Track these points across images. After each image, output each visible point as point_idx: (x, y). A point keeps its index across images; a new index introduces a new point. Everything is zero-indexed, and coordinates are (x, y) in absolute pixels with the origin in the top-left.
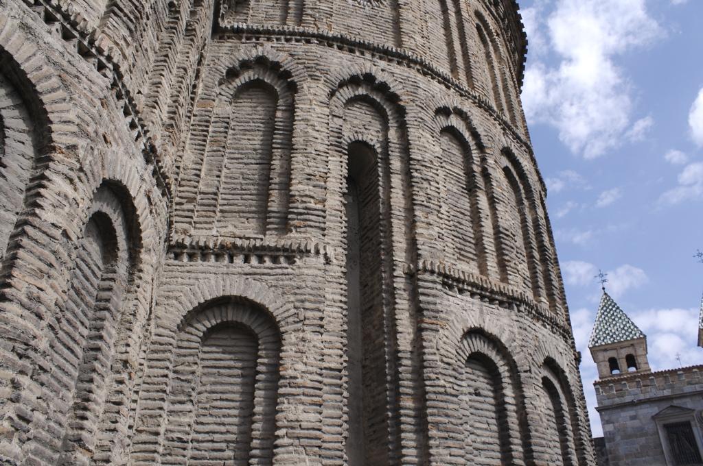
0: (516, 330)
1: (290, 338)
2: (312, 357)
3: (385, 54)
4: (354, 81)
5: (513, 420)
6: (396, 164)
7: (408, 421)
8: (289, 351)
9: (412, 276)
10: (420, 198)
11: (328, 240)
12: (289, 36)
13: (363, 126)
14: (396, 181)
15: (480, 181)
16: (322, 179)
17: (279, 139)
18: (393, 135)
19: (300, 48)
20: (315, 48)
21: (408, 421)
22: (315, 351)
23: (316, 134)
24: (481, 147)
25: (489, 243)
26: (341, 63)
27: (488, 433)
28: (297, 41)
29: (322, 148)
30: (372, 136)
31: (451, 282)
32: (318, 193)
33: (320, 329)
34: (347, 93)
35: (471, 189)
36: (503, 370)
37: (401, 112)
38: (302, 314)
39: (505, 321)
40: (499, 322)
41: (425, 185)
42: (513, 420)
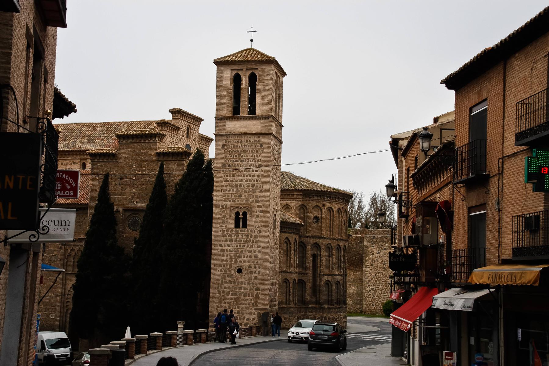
9: (320, 275)
11: (310, 272)
16: (310, 260)
19: (307, 239)
22: (309, 285)
25: (331, 266)
26: (312, 241)
27: (326, 292)
31: (324, 275)
37: (320, 248)
40: (330, 279)
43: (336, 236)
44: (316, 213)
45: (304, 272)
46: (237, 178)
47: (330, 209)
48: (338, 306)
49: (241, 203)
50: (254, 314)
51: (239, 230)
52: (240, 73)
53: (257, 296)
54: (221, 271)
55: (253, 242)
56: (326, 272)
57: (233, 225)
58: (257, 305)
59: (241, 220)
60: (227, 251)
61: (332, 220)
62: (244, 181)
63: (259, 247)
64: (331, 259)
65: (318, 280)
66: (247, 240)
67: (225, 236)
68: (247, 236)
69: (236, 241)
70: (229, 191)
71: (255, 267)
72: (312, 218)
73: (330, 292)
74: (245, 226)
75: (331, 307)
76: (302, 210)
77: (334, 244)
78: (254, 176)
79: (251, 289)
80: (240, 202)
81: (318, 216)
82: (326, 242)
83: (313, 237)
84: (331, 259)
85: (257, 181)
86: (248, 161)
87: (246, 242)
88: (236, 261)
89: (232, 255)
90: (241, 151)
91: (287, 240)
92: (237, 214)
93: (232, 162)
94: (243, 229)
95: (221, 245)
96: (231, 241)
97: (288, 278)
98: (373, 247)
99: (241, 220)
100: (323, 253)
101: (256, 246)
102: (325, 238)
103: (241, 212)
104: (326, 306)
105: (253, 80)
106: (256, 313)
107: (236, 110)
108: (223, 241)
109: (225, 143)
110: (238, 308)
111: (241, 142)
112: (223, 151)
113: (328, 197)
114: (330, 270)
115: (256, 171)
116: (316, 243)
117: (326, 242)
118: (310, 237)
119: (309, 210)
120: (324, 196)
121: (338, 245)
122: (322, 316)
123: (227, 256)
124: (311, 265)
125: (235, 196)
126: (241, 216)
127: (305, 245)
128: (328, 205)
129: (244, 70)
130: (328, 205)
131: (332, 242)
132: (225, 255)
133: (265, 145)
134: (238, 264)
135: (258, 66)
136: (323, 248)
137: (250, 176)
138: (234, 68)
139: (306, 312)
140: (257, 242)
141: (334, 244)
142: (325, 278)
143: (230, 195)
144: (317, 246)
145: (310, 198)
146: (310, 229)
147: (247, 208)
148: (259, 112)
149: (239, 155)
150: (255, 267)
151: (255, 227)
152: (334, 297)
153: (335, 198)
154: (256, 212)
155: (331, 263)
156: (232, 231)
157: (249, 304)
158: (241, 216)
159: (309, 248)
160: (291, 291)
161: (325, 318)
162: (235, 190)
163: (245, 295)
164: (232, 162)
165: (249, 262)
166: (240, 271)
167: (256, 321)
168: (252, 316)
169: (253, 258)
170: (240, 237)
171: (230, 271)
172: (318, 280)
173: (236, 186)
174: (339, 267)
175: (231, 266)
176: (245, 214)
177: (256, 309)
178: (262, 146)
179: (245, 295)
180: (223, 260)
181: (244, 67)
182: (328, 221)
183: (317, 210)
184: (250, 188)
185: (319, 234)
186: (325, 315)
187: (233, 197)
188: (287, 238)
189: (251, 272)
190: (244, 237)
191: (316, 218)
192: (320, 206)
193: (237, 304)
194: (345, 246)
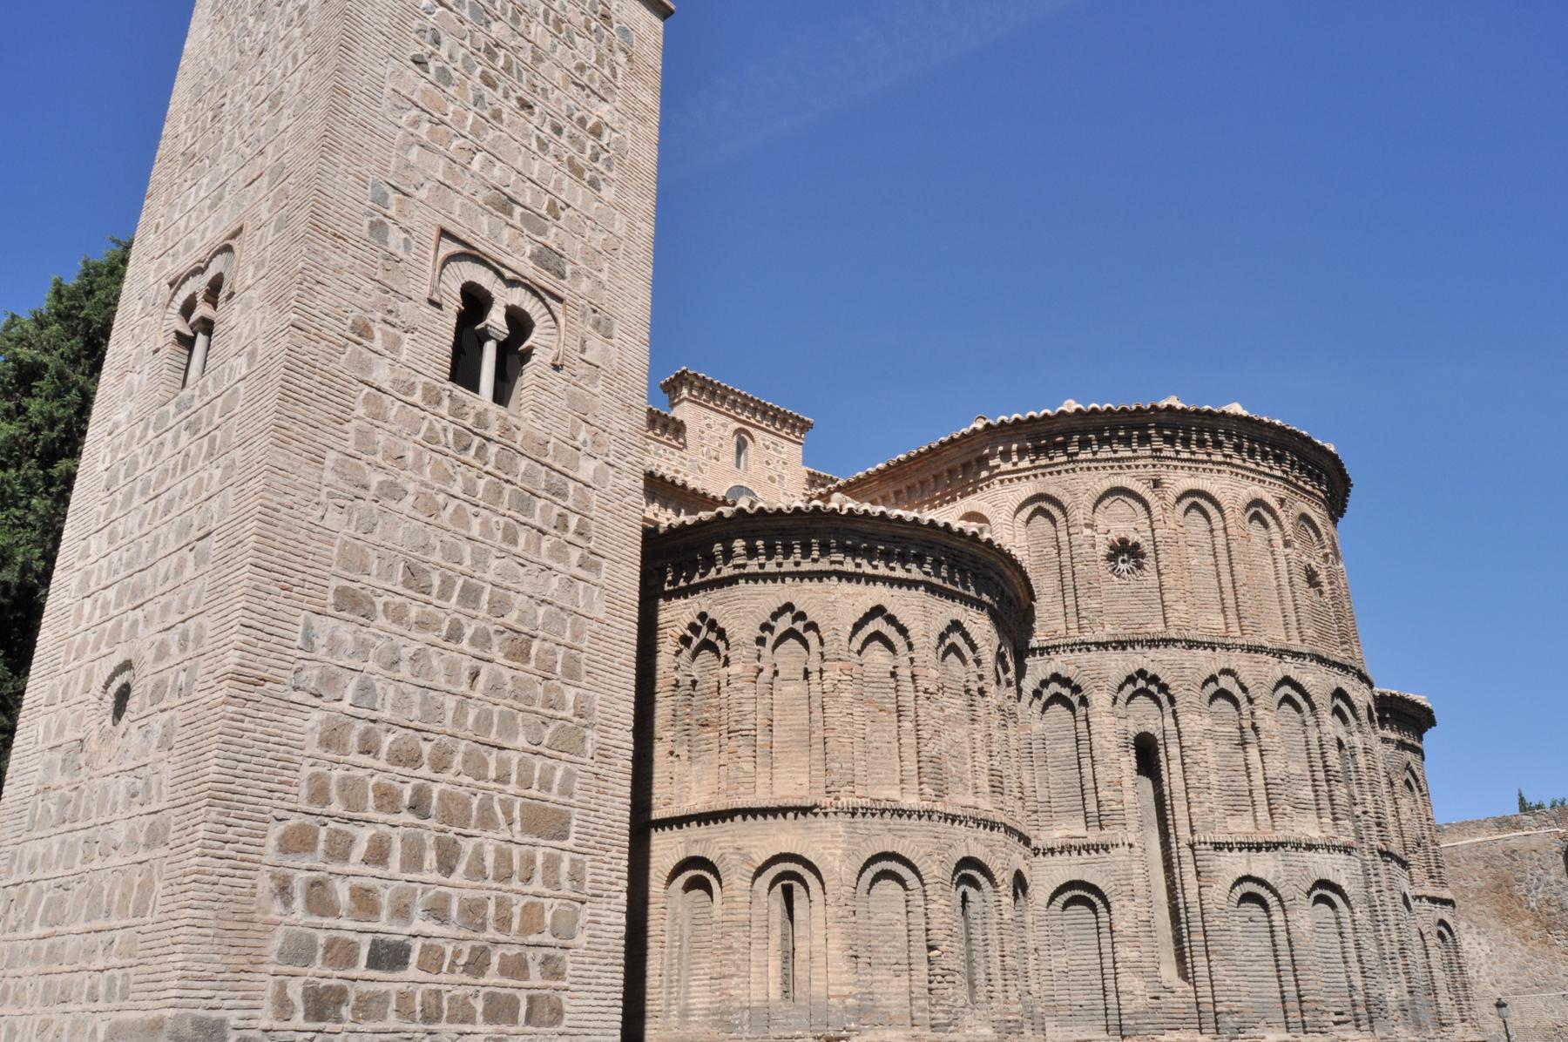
0: (1281, 868)
1: (1115, 906)
2: (1130, 917)
3: (1153, 643)
4: (1130, 679)
6: (1174, 750)
10: (1192, 782)
12: (1072, 647)
13: (1146, 717)
14: (1175, 766)
17: (1083, 746)
18: (1169, 720)
19: (1082, 657)
20: (1095, 655)
23: (1107, 745)
24: (1250, 701)
25: (1260, 796)
26: (1119, 664)
29: (1114, 756)
30: (1152, 727)
31: (1218, 847)
32: (1116, 796)
33: (1132, 897)
34: (1130, 689)
37: (1172, 700)
38: (1120, 889)
39: (1271, 863)
40: (1264, 866)
41: (1196, 768)
42: (1281, 938)
44: (1121, 522)
45: (1094, 836)
47: (1197, 501)
56: (1241, 827)
64: (1253, 752)
72: (1103, 550)
73: (1285, 957)
77: (1260, 673)
81: (1133, 537)
82: (1206, 662)
83: (1122, 645)
84: (1253, 752)
100: (1195, 723)
102: (1192, 644)
114: (1262, 813)
116: (1142, 673)
117: (1206, 662)
119: (1079, 515)
124: (1128, 797)
127: (1077, 689)
128: (1180, 480)
130: (1180, 480)
131: (1239, 661)
136: (1188, 695)
142: (1236, 864)
144: (1147, 686)
146: (1094, 604)
155: (1258, 780)
159: (1100, 700)
182: (1200, 560)
183: (1120, 507)
185: (1156, 628)
191: (1124, 551)
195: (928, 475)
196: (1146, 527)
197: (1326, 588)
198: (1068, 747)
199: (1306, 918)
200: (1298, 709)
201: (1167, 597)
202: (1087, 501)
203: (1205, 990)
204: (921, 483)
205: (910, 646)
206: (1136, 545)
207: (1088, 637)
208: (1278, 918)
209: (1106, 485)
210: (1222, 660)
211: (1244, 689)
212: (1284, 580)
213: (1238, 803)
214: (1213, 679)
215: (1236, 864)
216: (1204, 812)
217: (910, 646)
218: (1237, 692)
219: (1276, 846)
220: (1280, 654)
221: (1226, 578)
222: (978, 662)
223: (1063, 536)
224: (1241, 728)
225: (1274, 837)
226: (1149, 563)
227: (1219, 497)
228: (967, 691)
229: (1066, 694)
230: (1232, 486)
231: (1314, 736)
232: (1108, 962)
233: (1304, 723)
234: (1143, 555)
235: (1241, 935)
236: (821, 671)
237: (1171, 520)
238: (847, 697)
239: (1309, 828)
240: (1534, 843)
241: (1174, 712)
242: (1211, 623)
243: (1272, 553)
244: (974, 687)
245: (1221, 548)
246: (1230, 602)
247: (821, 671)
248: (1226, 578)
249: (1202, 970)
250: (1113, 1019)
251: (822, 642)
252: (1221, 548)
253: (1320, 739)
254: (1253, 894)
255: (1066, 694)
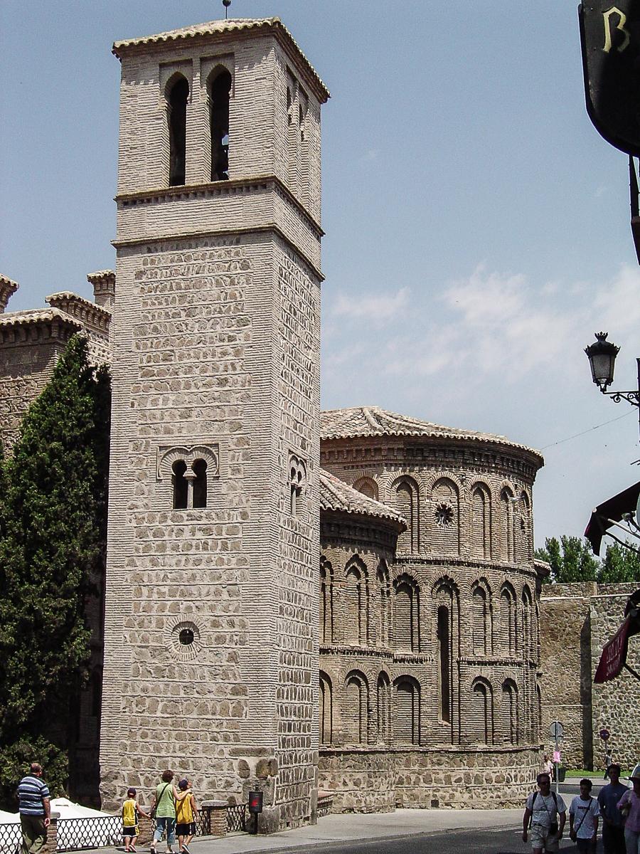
4: (440, 579)
5: (489, 704)
6: (456, 616)
7: (456, 707)
8: (423, 692)
13: (446, 600)
15: (488, 611)
16: (430, 624)
17: (414, 614)
18: (455, 601)
20: (425, 566)
21: (456, 707)
22: (431, 691)
24: (491, 593)
28: (419, 563)
31: (470, 663)
35: (485, 613)
36: (487, 688)
37: (458, 592)
40: (487, 672)
42: (489, 704)
43: (505, 561)
44: (443, 497)
45: (416, 655)
46: (175, 360)
47: (480, 488)
48: (510, 746)
49: (191, 434)
50: (231, 768)
51: (183, 513)
52: (185, 72)
53: (238, 712)
54: (133, 639)
55: (225, 548)
57: (170, 503)
58: (237, 739)
59: (191, 488)
60: (150, 580)
61: (488, 517)
62: (197, 371)
63: (242, 561)
64: (489, 618)
65: (456, 676)
66: (206, 543)
67: (141, 535)
68: (207, 531)
69: (176, 548)
70: (155, 402)
71: (232, 624)
72: (434, 510)
73: (489, 712)
74: (201, 502)
75: (493, 748)
76: (404, 492)
77: (496, 579)
78: (224, 354)
79: (220, 691)
80: (184, 432)
81: (449, 505)
82: (476, 573)
83: (437, 562)
84: (489, 618)
85: (234, 369)
86: (209, 313)
87: (205, 549)
88: (175, 608)
89: (165, 589)
90: (187, 288)
91: (355, 564)
92: (179, 467)
93: (162, 320)
94: (196, 512)
95: (132, 563)
96: (162, 548)
97: (363, 668)
98: (611, 620)
99: (190, 484)
100: (467, 603)
101: (234, 561)
102: (470, 564)
103: (189, 460)
104: (481, 746)
105: (221, 87)
106: (236, 764)
107: (177, 176)
108: (137, 550)
109: (142, 268)
110: (181, 749)
111: (189, 258)
112: (136, 291)
113: (473, 455)
114: (489, 646)
115: (231, 339)
116: (446, 577)
117: (476, 573)
118: (429, 562)
119: (425, 490)
120: (463, 453)
121: (507, 583)
122: (467, 775)
123: (151, 591)
125: (172, 416)
126: (189, 473)
128: (474, 477)
129: (196, 62)
131: (488, 574)
132: (145, 590)
133: (256, 264)
134: (182, 618)
135: (236, 47)
136: (465, 589)
137: (214, 355)
138: (168, 60)
139: (423, 765)
140: (235, 546)
141: (496, 579)
142: (475, 671)
143: (158, 413)
144: (447, 585)
145: (424, 459)
146: (427, 539)
147: (204, 449)
148: (236, 173)
149: (182, 297)
150: (232, 624)
151: (231, 501)
152: (502, 723)
153: (494, 457)
154: (234, 457)
155: (489, 631)
156: (165, 517)
157: (214, 739)
158: (189, 473)
159: (426, 590)
160: (373, 705)
161: (477, 778)
162: (172, 398)
163: (203, 709)
164: (162, 320)
165: (212, 608)
166: (187, 638)
167: (234, 788)
168: (221, 777)
169: (225, 596)
170: (187, 535)
171: (159, 640)
172: (456, 676)
173: (175, 388)
174: (514, 643)
175: (160, 624)
176: (200, 466)
177: (235, 753)
178: (245, 266)
179: (203, 709)
180: (137, 607)
181: (195, 55)
182: (477, 519)
183: (444, 488)
184: (215, 388)
185: (454, 555)
186: (475, 771)
187: (167, 419)
188: (356, 558)
189: (220, 639)
190: (199, 535)
191: (444, 513)
192: (454, 478)
193: (178, 738)
194: (526, 588)
195: (344, 449)
196: (455, 500)
197: (526, 529)
198: (407, 610)
199: (500, 696)
200: (508, 597)
201: (462, 539)
202: (429, 483)
203: (456, 726)
204: (338, 452)
205: (367, 575)
206: (450, 509)
207: (424, 557)
208: (489, 695)
209: (439, 475)
210: (481, 573)
211: (489, 587)
212: (511, 530)
213: (480, 641)
214: (477, 581)
215: (475, 671)
216: (467, 647)
217: (367, 575)
218: (486, 589)
219: (491, 663)
220: (505, 569)
221: (487, 529)
222: (388, 578)
223: (415, 499)
224: (485, 606)
225: (494, 658)
226: (454, 519)
227: (490, 486)
228: (382, 591)
229: (408, 585)
230: (495, 481)
231: (513, 609)
232: (416, 713)
233: (510, 603)
234: (452, 515)
235: (472, 703)
236: (332, 586)
237: (470, 501)
238: (343, 599)
239: (504, 655)
240: (567, 605)
241: (458, 598)
242: (478, 555)
243: (508, 514)
244: (385, 590)
245: (487, 513)
246: (488, 542)
247: (332, 586)
248: (487, 529)
249: (456, 717)
250: (416, 738)
251: (332, 572)
252: (487, 513)
253: (516, 611)
254: (481, 685)
255: (408, 585)
